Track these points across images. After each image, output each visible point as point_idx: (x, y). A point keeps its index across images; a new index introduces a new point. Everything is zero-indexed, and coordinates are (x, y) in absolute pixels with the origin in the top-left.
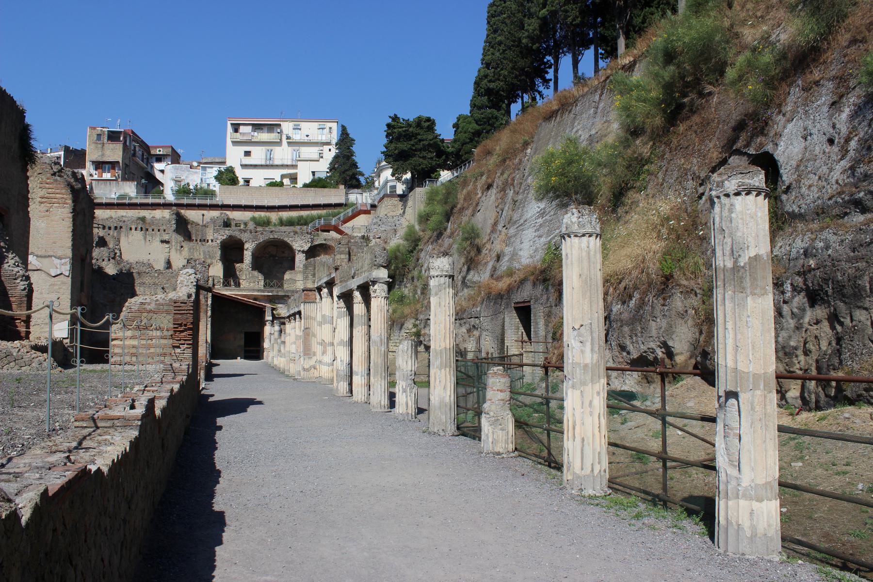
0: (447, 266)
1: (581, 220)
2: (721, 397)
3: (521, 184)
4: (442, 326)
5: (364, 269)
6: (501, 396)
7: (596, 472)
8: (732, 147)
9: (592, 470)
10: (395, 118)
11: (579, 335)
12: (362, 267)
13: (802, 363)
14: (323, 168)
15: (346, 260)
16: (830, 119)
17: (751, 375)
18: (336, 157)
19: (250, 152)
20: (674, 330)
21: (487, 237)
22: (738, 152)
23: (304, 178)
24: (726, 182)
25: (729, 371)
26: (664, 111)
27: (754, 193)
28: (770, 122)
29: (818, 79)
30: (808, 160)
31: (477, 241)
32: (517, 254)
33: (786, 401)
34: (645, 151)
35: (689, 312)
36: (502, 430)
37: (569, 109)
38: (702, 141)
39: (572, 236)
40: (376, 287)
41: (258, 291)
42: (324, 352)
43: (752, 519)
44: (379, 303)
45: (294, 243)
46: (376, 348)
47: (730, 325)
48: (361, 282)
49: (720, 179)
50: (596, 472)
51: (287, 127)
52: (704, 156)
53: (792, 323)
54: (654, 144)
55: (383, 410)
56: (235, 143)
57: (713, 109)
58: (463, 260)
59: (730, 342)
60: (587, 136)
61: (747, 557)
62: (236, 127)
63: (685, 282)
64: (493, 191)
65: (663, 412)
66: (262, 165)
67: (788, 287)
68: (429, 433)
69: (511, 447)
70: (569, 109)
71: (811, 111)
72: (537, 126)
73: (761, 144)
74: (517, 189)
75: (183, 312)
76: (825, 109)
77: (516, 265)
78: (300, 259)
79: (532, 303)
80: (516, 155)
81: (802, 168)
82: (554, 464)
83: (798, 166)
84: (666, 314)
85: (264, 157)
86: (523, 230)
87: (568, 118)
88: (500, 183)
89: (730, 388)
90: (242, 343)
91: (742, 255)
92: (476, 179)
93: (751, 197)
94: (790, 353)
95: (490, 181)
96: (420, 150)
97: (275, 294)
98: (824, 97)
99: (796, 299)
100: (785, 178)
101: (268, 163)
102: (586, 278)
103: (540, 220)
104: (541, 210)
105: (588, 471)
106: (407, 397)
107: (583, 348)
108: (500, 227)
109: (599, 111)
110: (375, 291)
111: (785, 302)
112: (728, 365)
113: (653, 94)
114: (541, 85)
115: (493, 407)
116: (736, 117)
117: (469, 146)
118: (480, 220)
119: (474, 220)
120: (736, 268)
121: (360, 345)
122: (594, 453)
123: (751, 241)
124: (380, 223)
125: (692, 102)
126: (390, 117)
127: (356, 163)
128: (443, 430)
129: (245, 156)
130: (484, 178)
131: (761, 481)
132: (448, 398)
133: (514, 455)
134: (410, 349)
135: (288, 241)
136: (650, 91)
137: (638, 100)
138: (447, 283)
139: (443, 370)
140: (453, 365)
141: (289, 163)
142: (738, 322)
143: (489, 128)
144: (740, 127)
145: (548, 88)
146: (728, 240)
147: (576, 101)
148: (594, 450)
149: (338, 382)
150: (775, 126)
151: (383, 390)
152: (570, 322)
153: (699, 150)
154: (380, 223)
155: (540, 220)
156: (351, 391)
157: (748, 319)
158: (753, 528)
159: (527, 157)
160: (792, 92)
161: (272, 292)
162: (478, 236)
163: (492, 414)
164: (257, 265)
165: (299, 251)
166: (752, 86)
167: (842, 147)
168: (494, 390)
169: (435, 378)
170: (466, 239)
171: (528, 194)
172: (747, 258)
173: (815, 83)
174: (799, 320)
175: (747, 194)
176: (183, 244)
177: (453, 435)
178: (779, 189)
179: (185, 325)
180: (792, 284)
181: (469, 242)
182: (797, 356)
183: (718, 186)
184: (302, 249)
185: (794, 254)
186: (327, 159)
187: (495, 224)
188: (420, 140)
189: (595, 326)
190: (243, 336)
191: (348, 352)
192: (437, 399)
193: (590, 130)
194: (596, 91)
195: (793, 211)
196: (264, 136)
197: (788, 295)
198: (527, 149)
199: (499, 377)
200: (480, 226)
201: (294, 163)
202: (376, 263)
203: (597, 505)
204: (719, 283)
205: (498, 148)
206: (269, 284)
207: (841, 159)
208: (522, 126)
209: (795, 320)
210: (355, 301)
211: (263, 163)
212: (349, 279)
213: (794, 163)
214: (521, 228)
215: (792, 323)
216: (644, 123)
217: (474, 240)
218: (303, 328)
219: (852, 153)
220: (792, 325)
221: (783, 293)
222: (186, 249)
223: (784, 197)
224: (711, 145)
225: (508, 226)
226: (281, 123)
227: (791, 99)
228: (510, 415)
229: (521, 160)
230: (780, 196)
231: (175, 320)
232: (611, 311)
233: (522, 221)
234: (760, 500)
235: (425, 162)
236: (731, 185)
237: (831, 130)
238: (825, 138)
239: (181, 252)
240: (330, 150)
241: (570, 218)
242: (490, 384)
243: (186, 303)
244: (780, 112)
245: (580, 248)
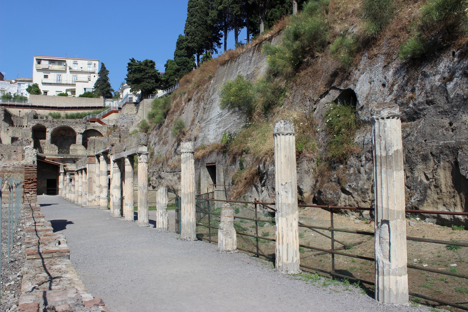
0: (191, 147)
1: (285, 126)
2: (379, 223)
3: (208, 99)
4: (188, 180)
5: (132, 146)
6: (229, 219)
7: (294, 261)
8: (331, 85)
9: (293, 261)
10: (133, 60)
11: (285, 188)
12: (131, 145)
13: (371, 197)
14: (90, 86)
15: (118, 141)
16: (383, 74)
17: (396, 211)
18: (98, 81)
19: (47, 76)
20: (303, 180)
21: (189, 128)
22: (334, 88)
23: (80, 91)
24: (382, 111)
25: (384, 210)
26: (293, 65)
27: (396, 118)
28: (351, 73)
29: (376, 53)
30: (372, 94)
31: (183, 129)
32: (206, 137)
33: (363, 216)
34: (283, 85)
35: (311, 170)
36: (230, 238)
37: (235, 60)
38: (314, 81)
39: (281, 134)
40: (141, 157)
41: (55, 155)
42: (101, 192)
43: (397, 285)
44: (142, 166)
45: (75, 129)
46: (141, 191)
47: (384, 186)
48: (131, 154)
49: (378, 110)
50: (294, 261)
51: (70, 62)
52: (316, 89)
53: (365, 177)
54: (287, 81)
55: (145, 225)
56: (38, 70)
57: (319, 65)
58: (175, 140)
59: (384, 194)
60: (246, 75)
61: (395, 305)
62: (39, 61)
63: (308, 155)
64: (192, 103)
65: (332, 229)
66: (54, 84)
67: (363, 158)
68: (181, 239)
69: (235, 247)
70: (235, 60)
71: (373, 70)
72: (216, 68)
73: (347, 84)
74: (205, 102)
75: (31, 172)
76: (381, 69)
77: (206, 143)
78: (79, 138)
79: (216, 164)
80: (205, 84)
81: (369, 98)
82: (272, 258)
83: (367, 97)
84: (299, 171)
85: (56, 79)
86: (209, 124)
87: (234, 64)
88: (196, 98)
89: (384, 218)
90: (46, 185)
91: (391, 150)
92: (181, 96)
93: (395, 120)
94: (364, 192)
95: (190, 97)
96: (147, 78)
97: (66, 157)
98: (380, 62)
99: (368, 165)
100: (360, 102)
101: (58, 82)
102: (288, 157)
103: (219, 119)
104: (220, 113)
105: (290, 261)
106: (163, 218)
107: (287, 195)
108: (196, 122)
109: (252, 62)
110: (140, 159)
111: (362, 166)
112: (384, 206)
113: (287, 55)
114: (216, 46)
115: (225, 226)
116: (332, 70)
117: (173, 77)
118: (184, 118)
119: (181, 118)
120: (387, 156)
121: (129, 189)
122: (293, 252)
123: (394, 142)
124: (124, 118)
125: (308, 61)
126: (130, 59)
127: (110, 84)
128: (189, 238)
129: (44, 78)
130: (186, 95)
131: (400, 266)
132: (192, 220)
133: (237, 251)
134: (164, 192)
135: (72, 128)
136: (285, 54)
137: (279, 57)
138: (191, 156)
139: (189, 204)
140: (194, 201)
141: (71, 83)
142: (389, 185)
143: (184, 67)
144: (335, 75)
145: (220, 48)
146: (383, 142)
147: (239, 56)
148: (293, 250)
149: (114, 209)
150: (354, 76)
151: (145, 214)
152: (280, 181)
153: (313, 86)
154: (124, 118)
155: (219, 119)
156: (122, 214)
157: (394, 183)
158: (397, 290)
159: (211, 85)
160: (363, 59)
161: (63, 156)
162: (184, 127)
163: (225, 229)
164: (54, 140)
165: (79, 133)
166: (343, 55)
167: (390, 89)
168: (226, 217)
169: (184, 209)
170: (177, 128)
171: (212, 105)
172: (393, 151)
173: (375, 55)
174: (369, 175)
175: (393, 118)
176: (9, 128)
177: (195, 240)
178: (357, 108)
179: (32, 180)
180: (365, 157)
181: (179, 130)
182: (368, 193)
183: (377, 113)
184: (80, 132)
185: (366, 142)
186: (93, 82)
187: (193, 120)
188: (147, 73)
189: (293, 183)
190: (46, 181)
191: (120, 192)
192: (186, 220)
193: (247, 72)
194: (250, 51)
195: (365, 120)
196: (56, 67)
197: (364, 162)
198: (211, 81)
199: (228, 209)
200: (184, 121)
201: (73, 83)
202: (141, 143)
203: (300, 279)
204: (377, 164)
205: (193, 79)
206: (62, 152)
207: (390, 95)
208: (207, 68)
209: (367, 175)
210: (126, 164)
211: (55, 82)
212: (121, 151)
213: (365, 95)
214: (208, 123)
215: (365, 177)
216: (282, 70)
217: (182, 129)
218: (88, 178)
219: (395, 92)
220: (366, 178)
221: (361, 161)
222: (11, 131)
223: (360, 112)
224: (319, 83)
225: (200, 122)
226: (66, 60)
227: (362, 63)
228: (234, 230)
229: (207, 86)
230: (357, 112)
231: (25, 177)
232: (268, 169)
233: (209, 119)
234: (400, 275)
235: (149, 85)
236: (385, 113)
237: (384, 80)
238: (381, 84)
239: (7, 133)
240: (95, 76)
241: (280, 125)
242: (223, 213)
243: (32, 167)
244: (357, 69)
245: (285, 141)
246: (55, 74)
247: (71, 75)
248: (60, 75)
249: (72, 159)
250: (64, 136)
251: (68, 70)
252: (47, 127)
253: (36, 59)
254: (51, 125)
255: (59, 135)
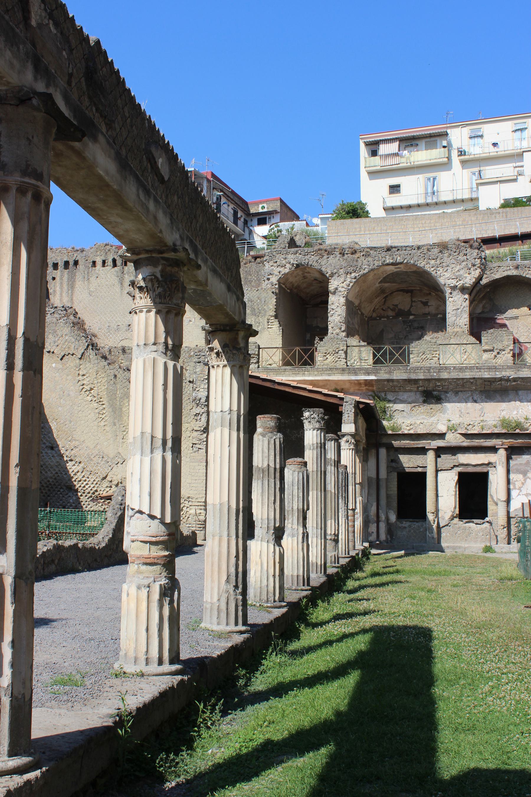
19: (398, 186)
56: (373, 174)
62: (373, 147)
66: (419, 206)
97: (386, 376)
101: (429, 200)
129: (391, 193)
135: (428, 268)
165: (454, 288)
184: (460, 284)
211: (422, 201)
226: (449, 131)
246: (420, 176)
247: (467, 173)
248: (434, 179)
249: (416, 381)
250: (409, 313)
251: (456, 160)
252: (332, 275)
253: (367, 144)
254: (344, 264)
255: (391, 313)
